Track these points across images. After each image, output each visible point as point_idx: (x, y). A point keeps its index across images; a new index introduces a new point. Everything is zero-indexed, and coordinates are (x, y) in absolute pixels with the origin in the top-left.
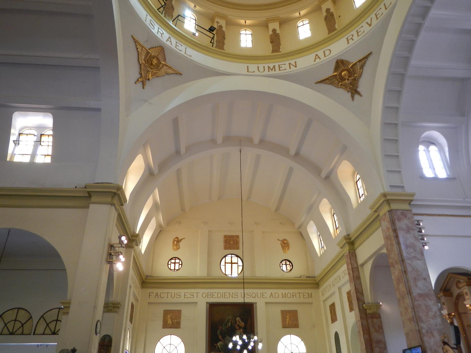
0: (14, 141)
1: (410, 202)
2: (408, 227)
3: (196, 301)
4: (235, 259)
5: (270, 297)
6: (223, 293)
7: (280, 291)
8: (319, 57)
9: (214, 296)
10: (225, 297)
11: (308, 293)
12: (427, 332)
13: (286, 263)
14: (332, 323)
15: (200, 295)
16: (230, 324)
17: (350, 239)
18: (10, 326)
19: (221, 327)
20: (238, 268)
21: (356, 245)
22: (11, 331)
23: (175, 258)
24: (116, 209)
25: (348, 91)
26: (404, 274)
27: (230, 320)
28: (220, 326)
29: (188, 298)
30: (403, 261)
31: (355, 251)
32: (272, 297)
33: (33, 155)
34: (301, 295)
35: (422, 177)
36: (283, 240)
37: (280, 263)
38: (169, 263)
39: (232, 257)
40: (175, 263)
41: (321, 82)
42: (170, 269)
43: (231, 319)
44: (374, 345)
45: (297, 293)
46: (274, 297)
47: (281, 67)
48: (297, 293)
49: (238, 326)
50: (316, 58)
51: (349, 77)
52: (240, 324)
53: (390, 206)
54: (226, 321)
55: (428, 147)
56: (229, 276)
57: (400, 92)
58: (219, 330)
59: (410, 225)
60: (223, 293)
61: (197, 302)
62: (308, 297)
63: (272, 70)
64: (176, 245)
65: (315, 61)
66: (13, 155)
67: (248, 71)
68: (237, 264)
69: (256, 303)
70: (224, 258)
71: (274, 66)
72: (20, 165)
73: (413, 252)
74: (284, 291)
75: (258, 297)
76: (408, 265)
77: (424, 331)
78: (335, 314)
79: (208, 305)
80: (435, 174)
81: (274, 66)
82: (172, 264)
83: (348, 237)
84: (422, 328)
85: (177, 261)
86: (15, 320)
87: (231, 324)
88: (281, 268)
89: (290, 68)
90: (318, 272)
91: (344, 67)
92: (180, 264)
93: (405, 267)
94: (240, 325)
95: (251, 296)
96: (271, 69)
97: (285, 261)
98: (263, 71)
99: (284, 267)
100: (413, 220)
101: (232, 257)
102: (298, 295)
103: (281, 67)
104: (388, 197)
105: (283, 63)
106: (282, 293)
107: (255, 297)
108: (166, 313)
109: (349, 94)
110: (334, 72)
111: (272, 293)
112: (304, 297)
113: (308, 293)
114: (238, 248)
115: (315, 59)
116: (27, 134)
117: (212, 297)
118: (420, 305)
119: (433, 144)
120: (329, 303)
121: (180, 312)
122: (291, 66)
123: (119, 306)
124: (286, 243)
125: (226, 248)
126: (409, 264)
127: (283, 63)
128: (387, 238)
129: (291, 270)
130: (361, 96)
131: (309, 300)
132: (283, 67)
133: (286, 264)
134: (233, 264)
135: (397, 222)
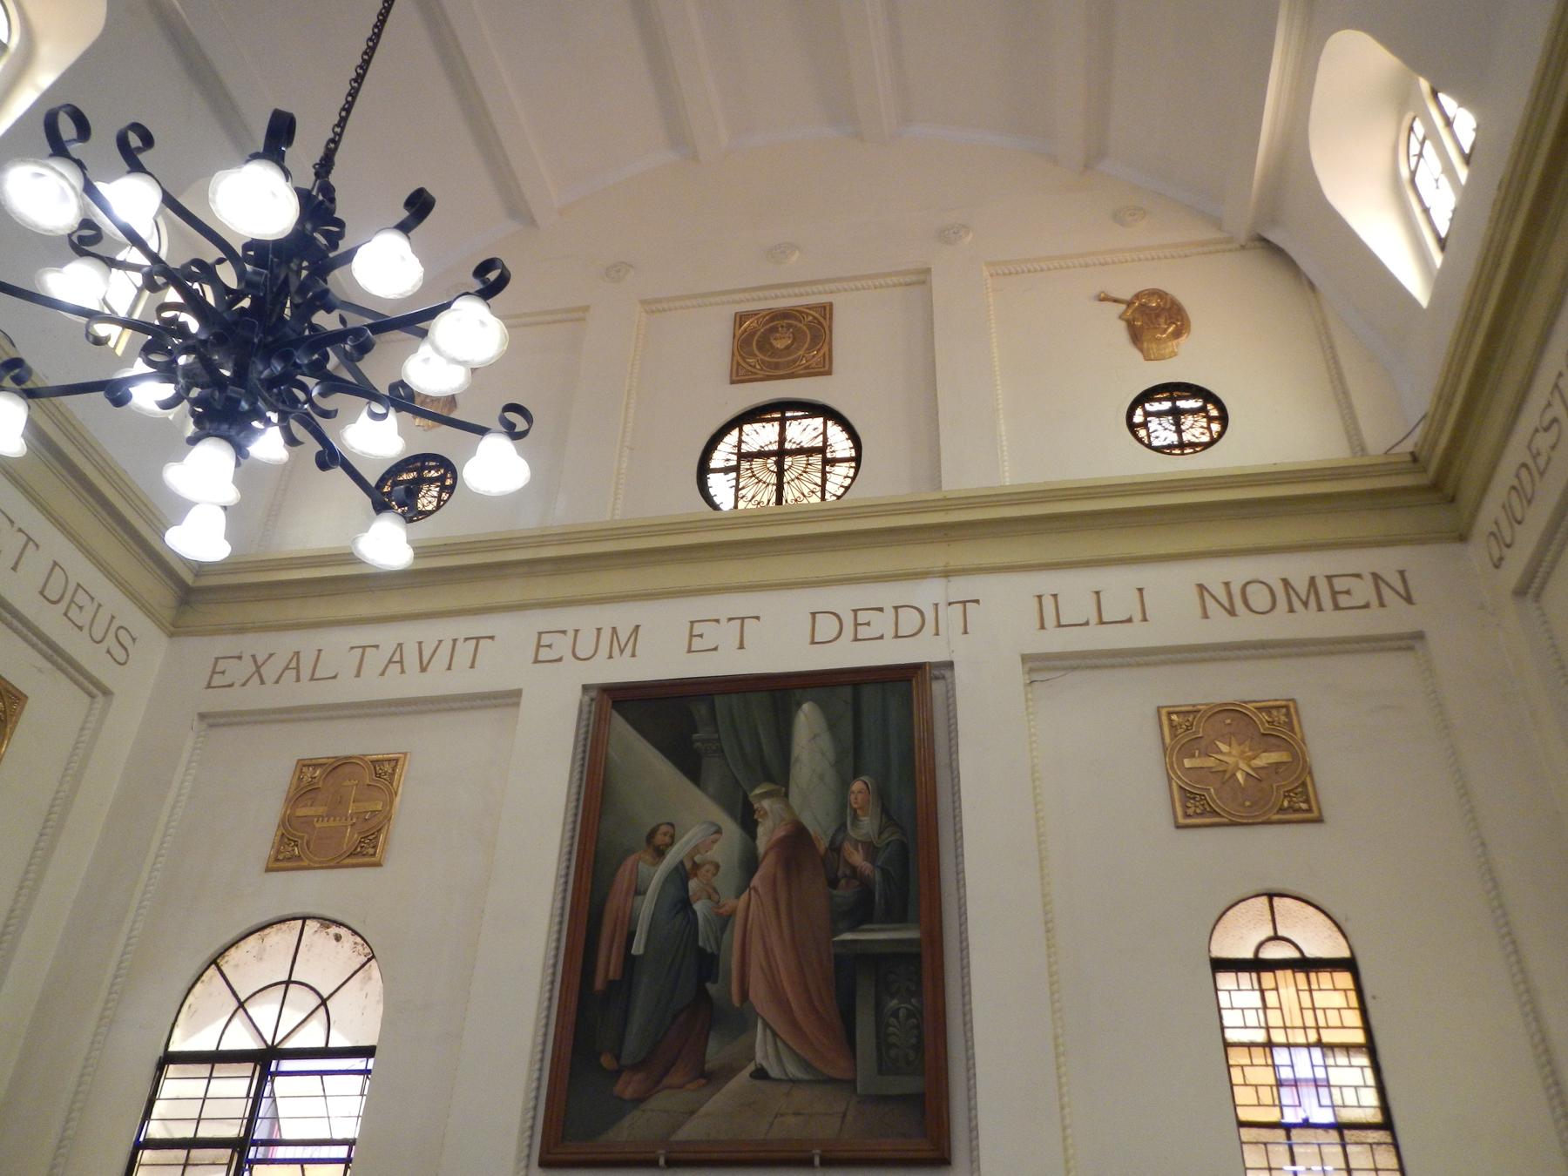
61: (518, 693)
62: (1375, 602)
70: (735, 432)
125: (740, 376)
131: (1394, 619)
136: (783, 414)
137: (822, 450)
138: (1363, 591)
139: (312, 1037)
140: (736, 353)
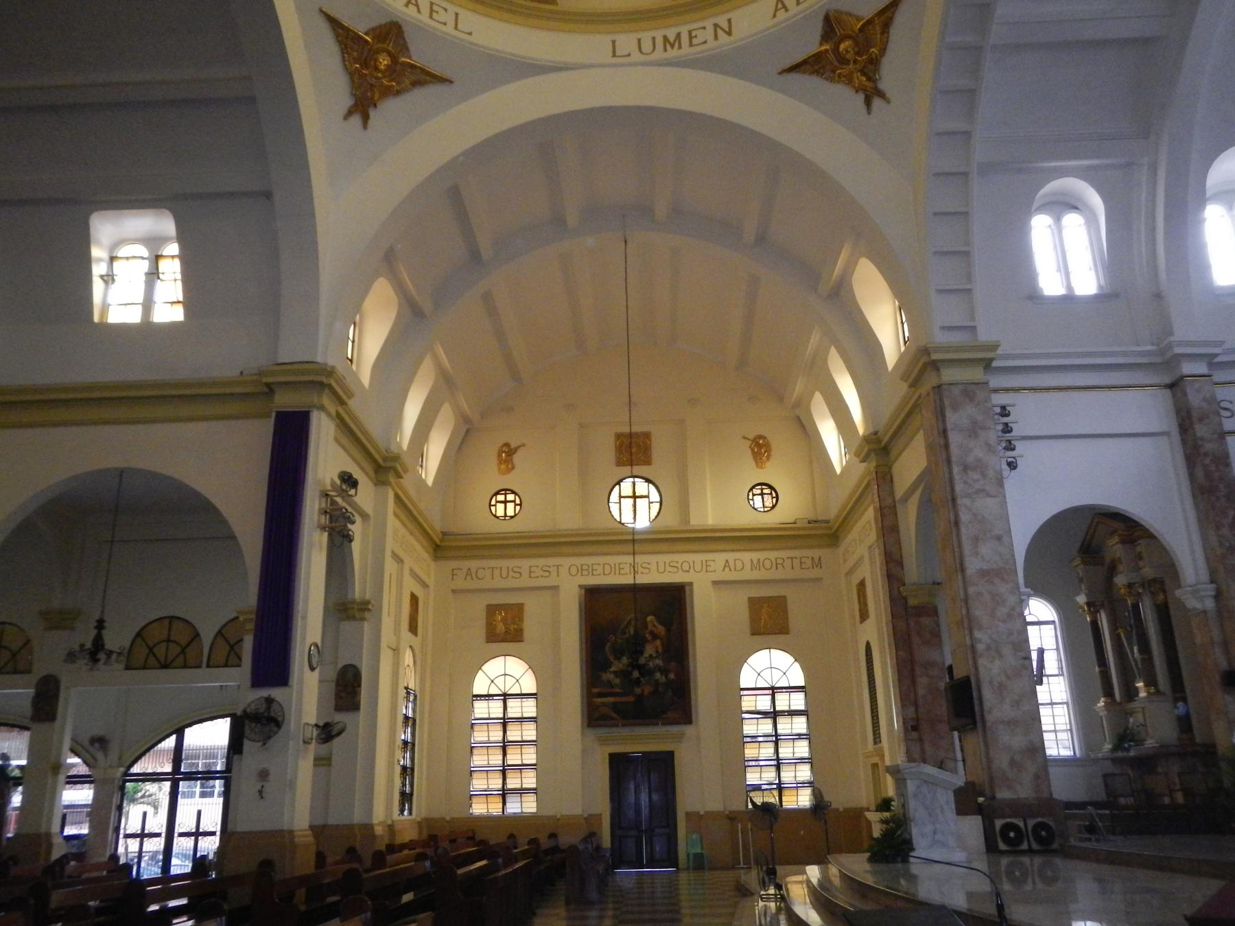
0: (102, 277)
1: (987, 364)
2: (974, 423)
3: (556, 584)
4: (642, 487)
5: (724, 570)
7: (747, 557)
8: (784, 7)
9: (595, 573)
10: (619, 574)
11: (812, 558)
12: (989, 648)
13: (762, 491)
14: (861, 623)
15: (563, 571)
16: (632, 631)
17: (879, 441)
18: (160, 651)
20: (650, 508)
21: (893, 454)
22: (162, 660)
23: (506, 491)
24: (329, 415)
25: (857, 91)
26: (954, 529)
27: (633, 622)
28: (611, 636)
30: (954, 500)
31: (890, 468)
32: (727, 569)
33: (148, 305)
34: (796, 562)
35: (1034, 296)
36: (755, 438)
37: (749, 492)
38: (493, 502)
39: (634, 484)
40: (505, 502)
41: (794, 68)
42: (495, 516)
44: (918, 671)
45: (788, 558)
46: (732, 568)
47: (696, 36)
48: (788, 558)
49: (652, 633)
50: (779, 8)
51: (858, 53)
52: (654, 629)
53: (939, 376)
55: (1058, 220)
56: (629, 525)
57: (972, 93)
58: (609, 644)
59: (980, 418)
62: (811, 566)
63: (672, 46)
64: (506, 461)
65: (775, 16)
66: (105, 308)
67: (614, 55)
68: (647, 499)
69: (691, 584)
70: (617, 487)
71: (678, 36)
72: (123, 330)
73: (978, 480)
74: (755, 556)
75: (696, 569)
76: (963, 508)
77: (980, 647)
78: (866, 605)
79: (583, 591)
80: (1069, 287)
81: (678, 36)
82: (498, 504)
83: (875, 437)
84: (980, 641)
85: (510, 497)
86: (168, 640)
87: (636, 631)
88: (751, 502)
89: (716, 37)
90: (833, 511)
91: (844, 30)
92: (518, 505)
93: (957, 516)
94: (656, 632)
95: (680, 567)
96: (670, 43)
97: (760, 487)
98: (651, 49)
99: (758, 502)
100: (990, 405)
101: (634, 484)
102: (788, 562)
103: (696, 36)
104: (935, 356)
105: (701, 24)
106: (752, 560)
107: (688, 571)
108: (492, 610)
109: (860, 98)
110: (821, 44)
111: (727, 561)
112: (803, 566)
113: (812, 558)
114: (647, 461)
115: (776, 10)
116: (127, 258)
117: (591, 574)
118: (980, 594)
119: (1074, 208)
120: (855, 580)
121: (520, 607)
122: (720, 32)
123: (370, 607)
124: (764, 445)
125: (619, 463)
126: (966, 506)
127: (701, 24)
128: (930, 448)
129: (774, 507)
130: (888, 102)
131: (815, 573)
132: (701, 36)
133: (762, 494)
134: (637, 500)
135: (949, 414)
137: (647, 497)
138: (809, 563)
139: (515, 690)
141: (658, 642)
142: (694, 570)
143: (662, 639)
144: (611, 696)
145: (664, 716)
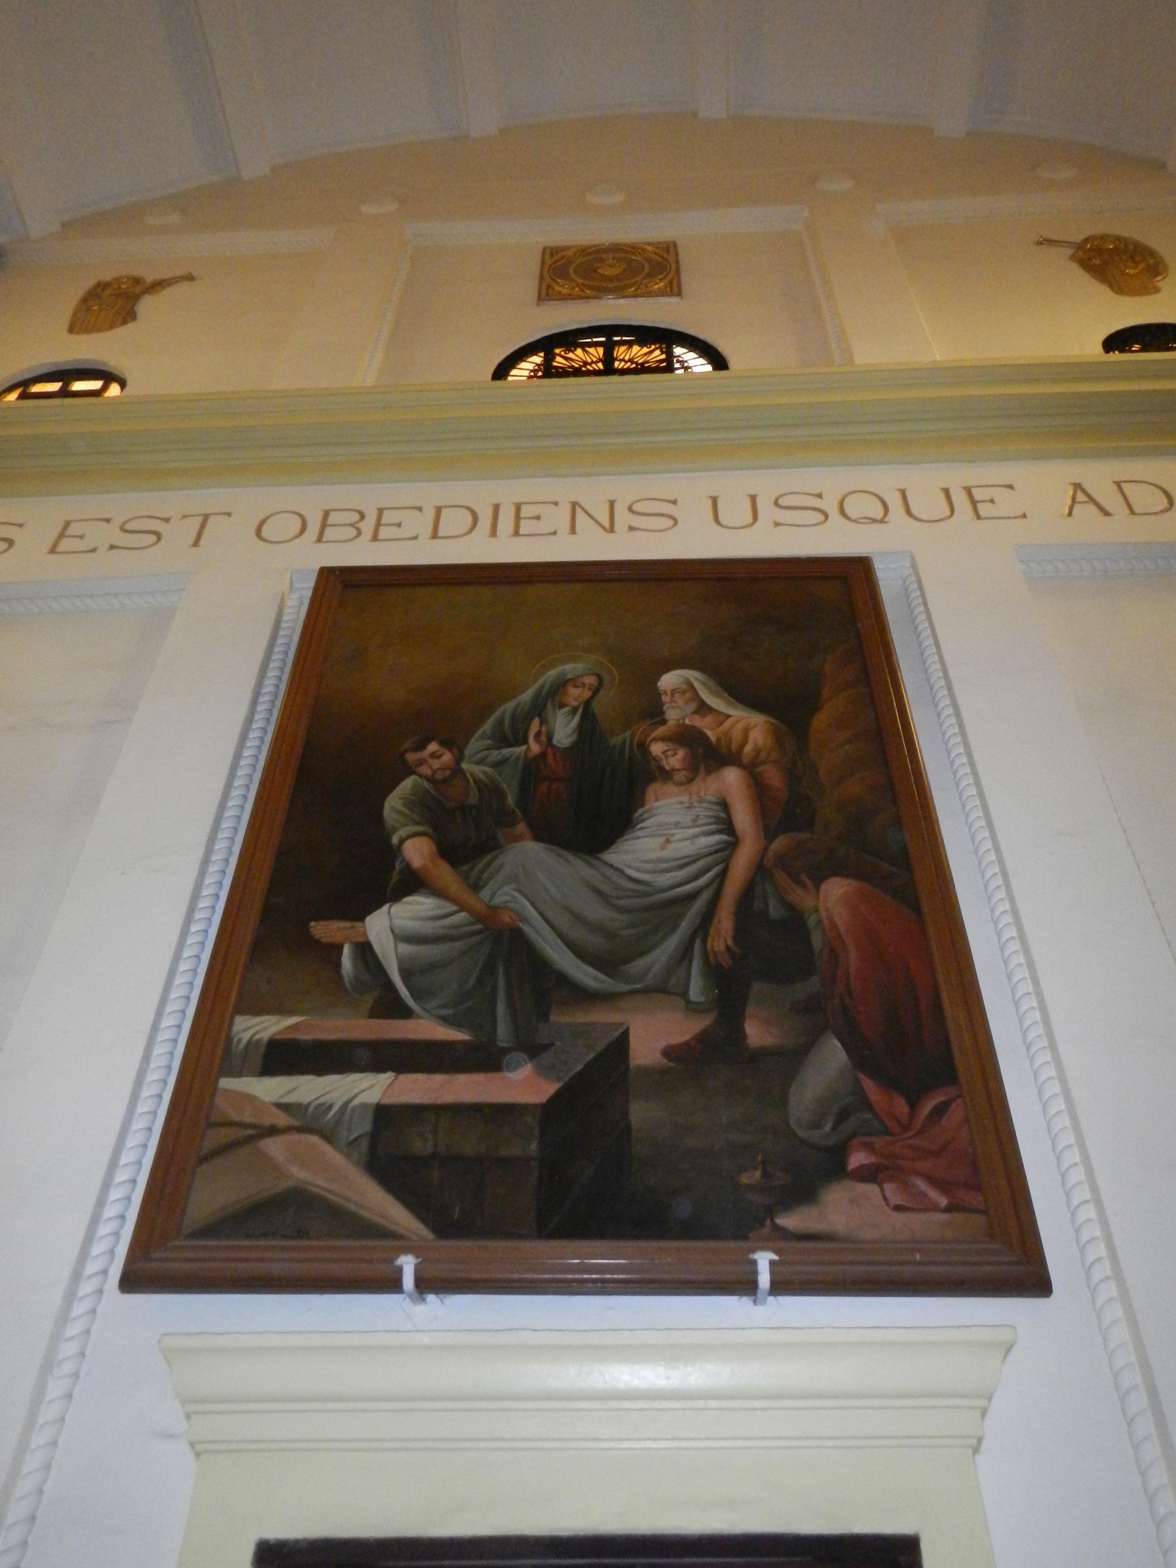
6: (496, 508)
16: (564, 730)
19: (433, 755)
28: (433, 747)
29: (94, 550)
43: (591, 680)
49: (688, 738)
52: (705, 725)
54: (510, 706)
60: (496, 508)
136: (609, 339)
140: (546, 275)
141: (732, 777)
142: (909, 512)
143: (751, 770)
144: (378, 1066)
145: (789, 1221)
